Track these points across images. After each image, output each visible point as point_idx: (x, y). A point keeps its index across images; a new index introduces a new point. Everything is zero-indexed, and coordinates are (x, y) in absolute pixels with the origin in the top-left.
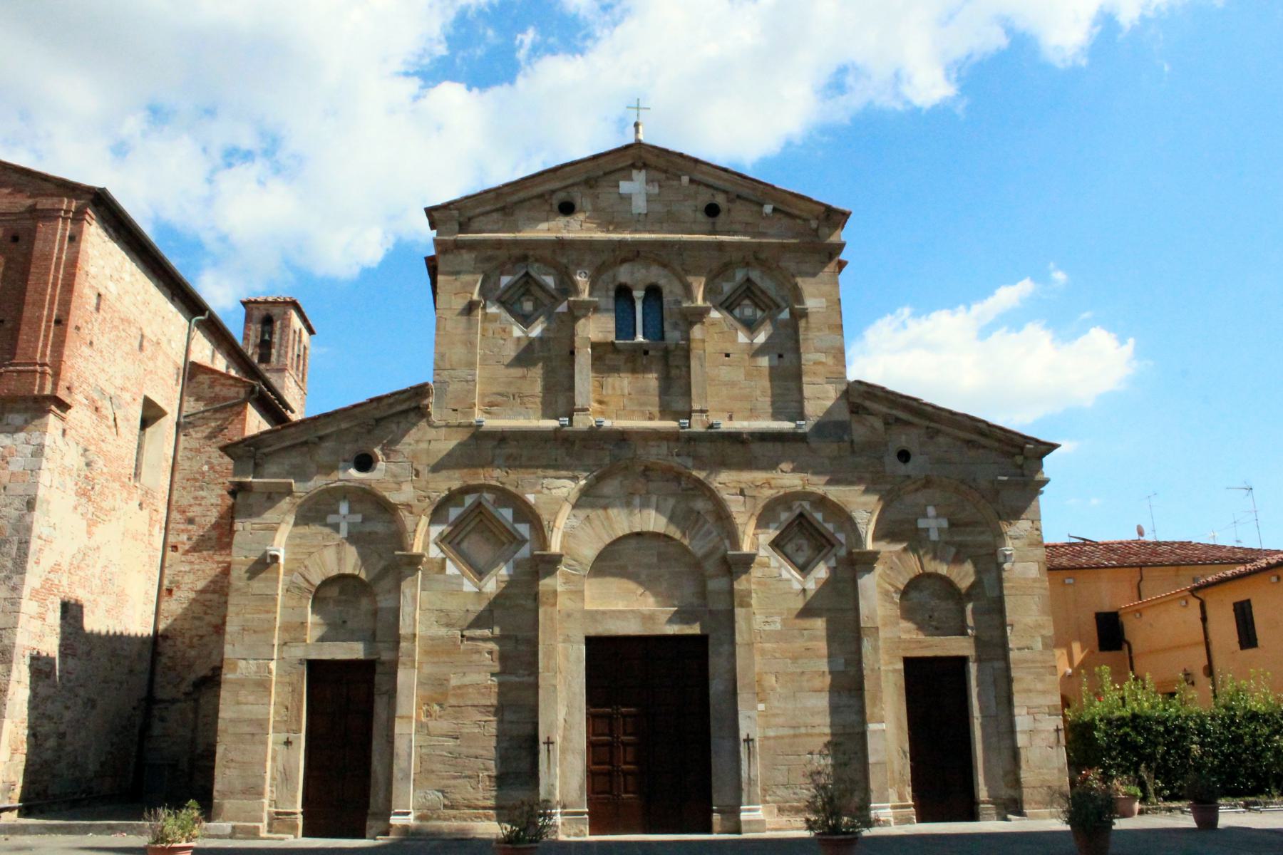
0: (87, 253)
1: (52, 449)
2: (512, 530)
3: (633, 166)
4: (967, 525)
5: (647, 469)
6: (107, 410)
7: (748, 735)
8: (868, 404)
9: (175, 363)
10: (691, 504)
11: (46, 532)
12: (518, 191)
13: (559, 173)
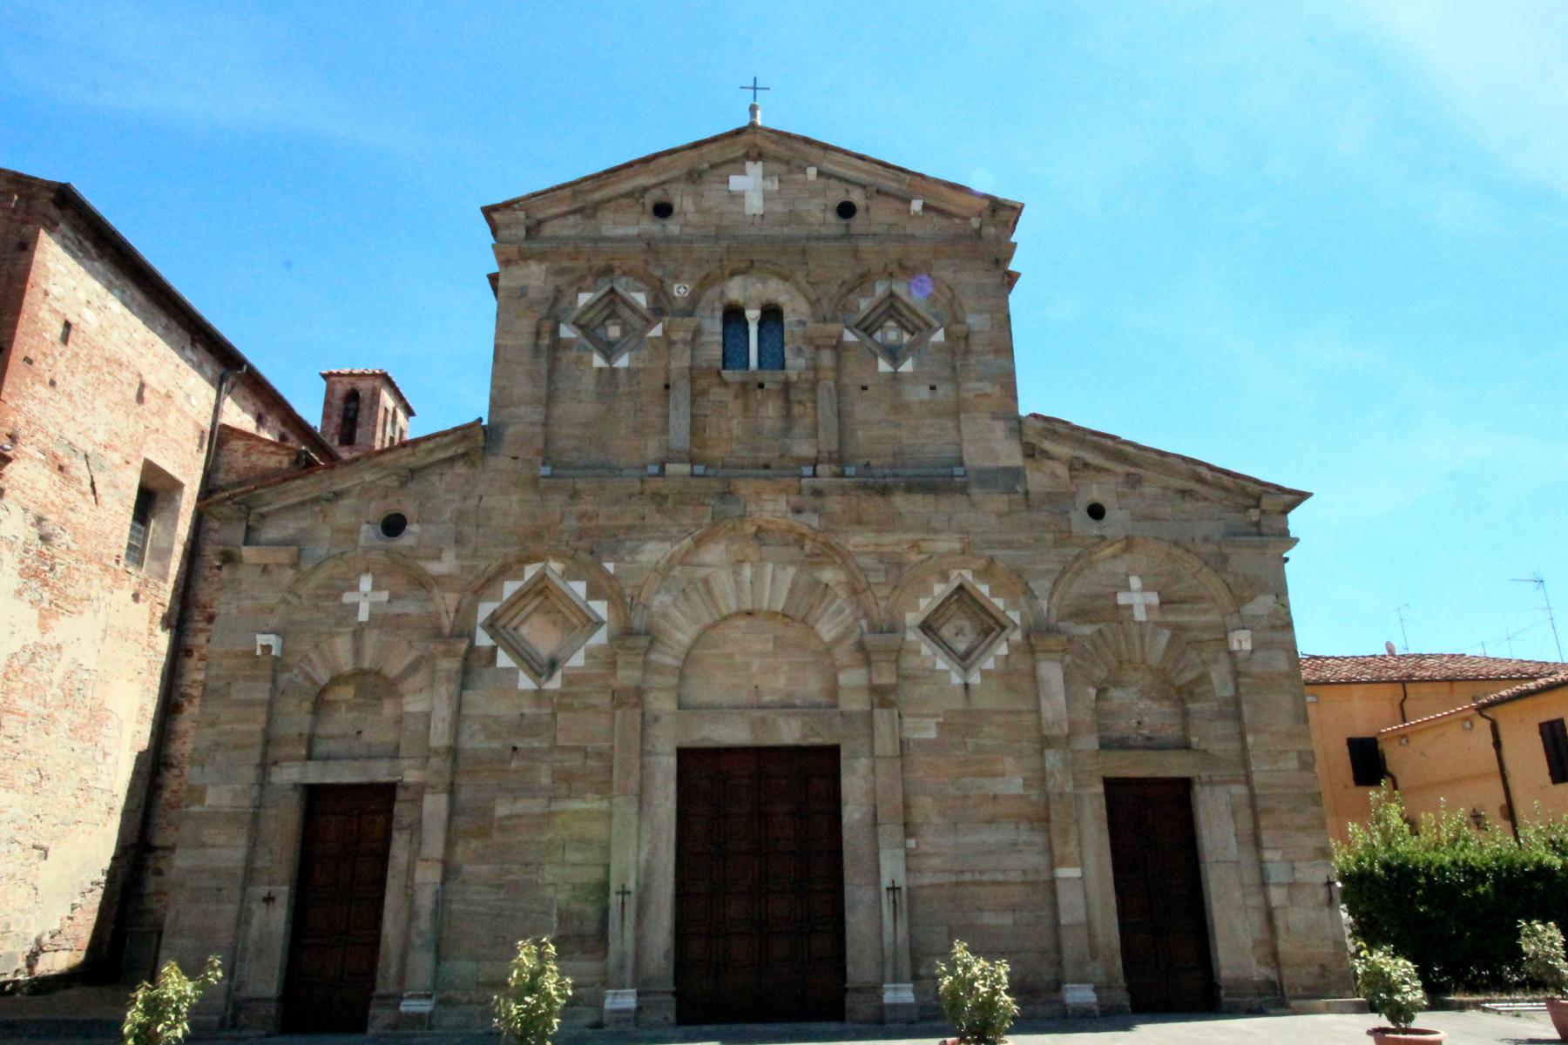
2: (585, 610)
3: (747, 157)
4: (1183, 601)
5: (760, 529)
6: (78, 468)
7: (893, 882)
8: (1048, 445)
9: (197, 424)
10: (817, 574)
12: (600, 187)
13: (652, 166)
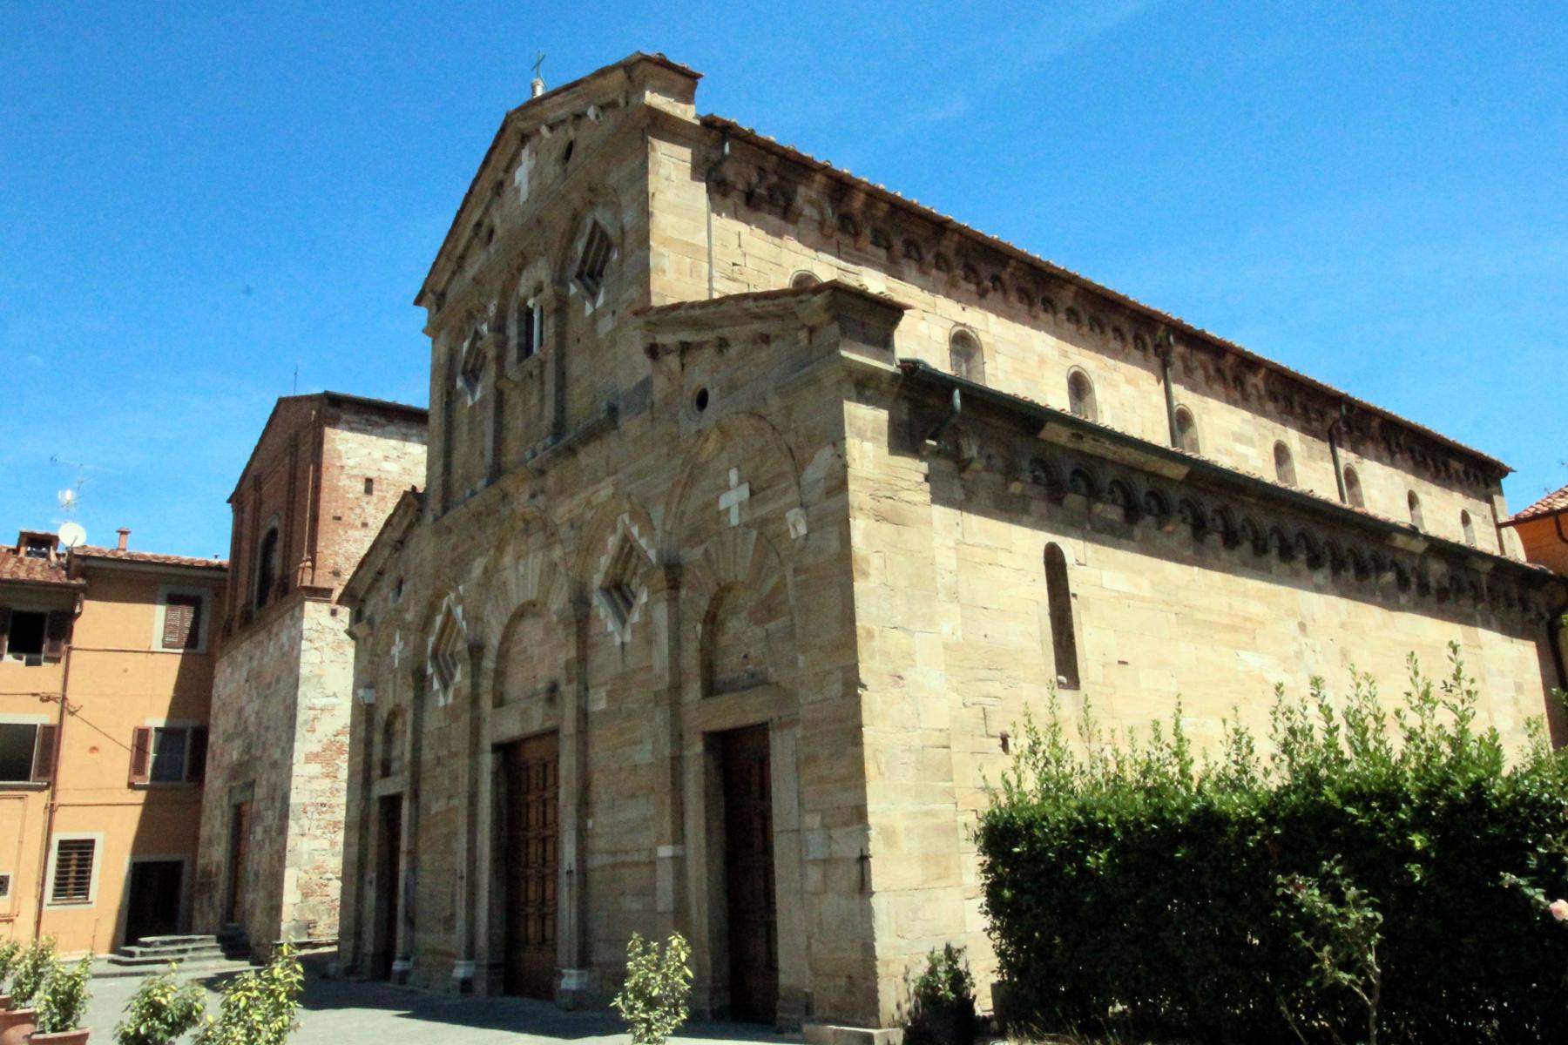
0: (336, 450)
1: (317, 631)
11: (320, 702)
12: (457, 241)
